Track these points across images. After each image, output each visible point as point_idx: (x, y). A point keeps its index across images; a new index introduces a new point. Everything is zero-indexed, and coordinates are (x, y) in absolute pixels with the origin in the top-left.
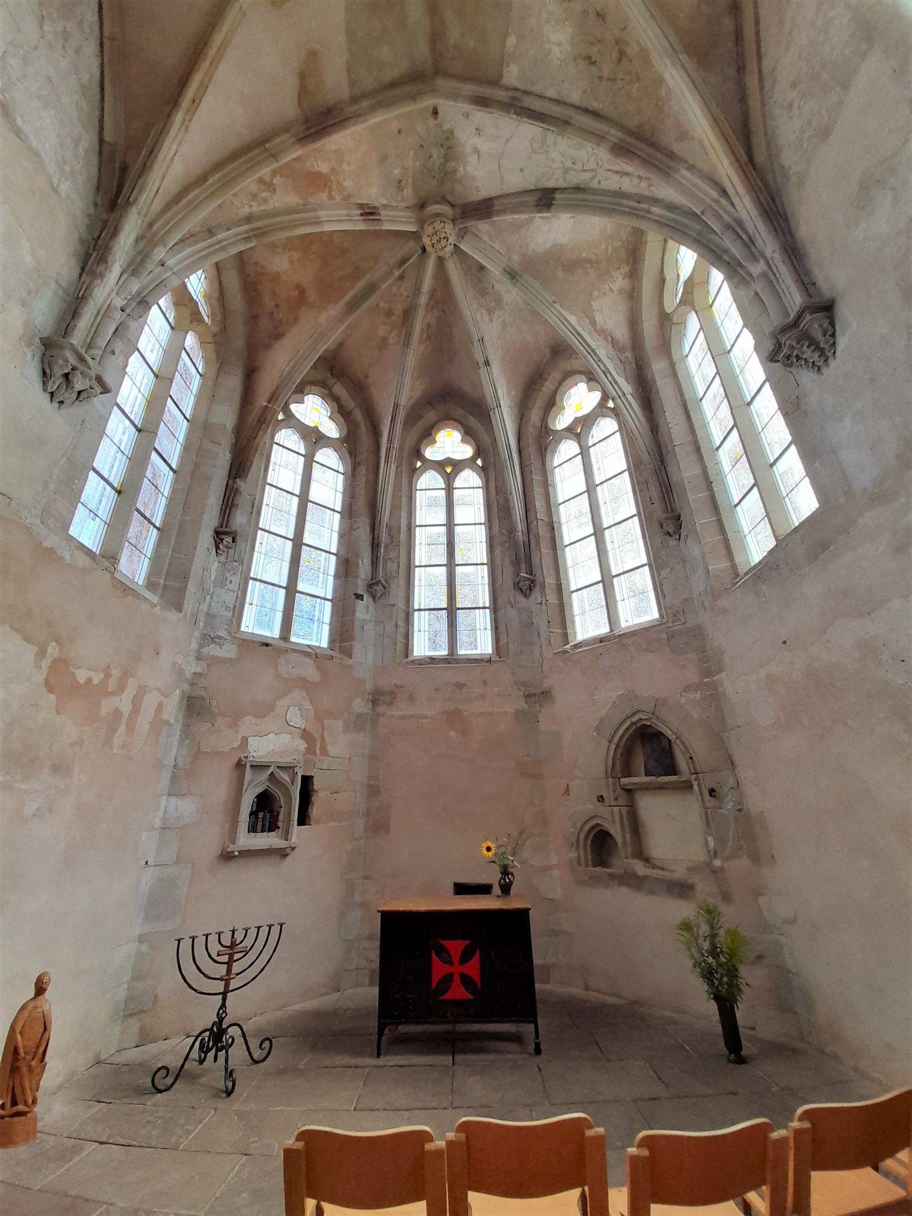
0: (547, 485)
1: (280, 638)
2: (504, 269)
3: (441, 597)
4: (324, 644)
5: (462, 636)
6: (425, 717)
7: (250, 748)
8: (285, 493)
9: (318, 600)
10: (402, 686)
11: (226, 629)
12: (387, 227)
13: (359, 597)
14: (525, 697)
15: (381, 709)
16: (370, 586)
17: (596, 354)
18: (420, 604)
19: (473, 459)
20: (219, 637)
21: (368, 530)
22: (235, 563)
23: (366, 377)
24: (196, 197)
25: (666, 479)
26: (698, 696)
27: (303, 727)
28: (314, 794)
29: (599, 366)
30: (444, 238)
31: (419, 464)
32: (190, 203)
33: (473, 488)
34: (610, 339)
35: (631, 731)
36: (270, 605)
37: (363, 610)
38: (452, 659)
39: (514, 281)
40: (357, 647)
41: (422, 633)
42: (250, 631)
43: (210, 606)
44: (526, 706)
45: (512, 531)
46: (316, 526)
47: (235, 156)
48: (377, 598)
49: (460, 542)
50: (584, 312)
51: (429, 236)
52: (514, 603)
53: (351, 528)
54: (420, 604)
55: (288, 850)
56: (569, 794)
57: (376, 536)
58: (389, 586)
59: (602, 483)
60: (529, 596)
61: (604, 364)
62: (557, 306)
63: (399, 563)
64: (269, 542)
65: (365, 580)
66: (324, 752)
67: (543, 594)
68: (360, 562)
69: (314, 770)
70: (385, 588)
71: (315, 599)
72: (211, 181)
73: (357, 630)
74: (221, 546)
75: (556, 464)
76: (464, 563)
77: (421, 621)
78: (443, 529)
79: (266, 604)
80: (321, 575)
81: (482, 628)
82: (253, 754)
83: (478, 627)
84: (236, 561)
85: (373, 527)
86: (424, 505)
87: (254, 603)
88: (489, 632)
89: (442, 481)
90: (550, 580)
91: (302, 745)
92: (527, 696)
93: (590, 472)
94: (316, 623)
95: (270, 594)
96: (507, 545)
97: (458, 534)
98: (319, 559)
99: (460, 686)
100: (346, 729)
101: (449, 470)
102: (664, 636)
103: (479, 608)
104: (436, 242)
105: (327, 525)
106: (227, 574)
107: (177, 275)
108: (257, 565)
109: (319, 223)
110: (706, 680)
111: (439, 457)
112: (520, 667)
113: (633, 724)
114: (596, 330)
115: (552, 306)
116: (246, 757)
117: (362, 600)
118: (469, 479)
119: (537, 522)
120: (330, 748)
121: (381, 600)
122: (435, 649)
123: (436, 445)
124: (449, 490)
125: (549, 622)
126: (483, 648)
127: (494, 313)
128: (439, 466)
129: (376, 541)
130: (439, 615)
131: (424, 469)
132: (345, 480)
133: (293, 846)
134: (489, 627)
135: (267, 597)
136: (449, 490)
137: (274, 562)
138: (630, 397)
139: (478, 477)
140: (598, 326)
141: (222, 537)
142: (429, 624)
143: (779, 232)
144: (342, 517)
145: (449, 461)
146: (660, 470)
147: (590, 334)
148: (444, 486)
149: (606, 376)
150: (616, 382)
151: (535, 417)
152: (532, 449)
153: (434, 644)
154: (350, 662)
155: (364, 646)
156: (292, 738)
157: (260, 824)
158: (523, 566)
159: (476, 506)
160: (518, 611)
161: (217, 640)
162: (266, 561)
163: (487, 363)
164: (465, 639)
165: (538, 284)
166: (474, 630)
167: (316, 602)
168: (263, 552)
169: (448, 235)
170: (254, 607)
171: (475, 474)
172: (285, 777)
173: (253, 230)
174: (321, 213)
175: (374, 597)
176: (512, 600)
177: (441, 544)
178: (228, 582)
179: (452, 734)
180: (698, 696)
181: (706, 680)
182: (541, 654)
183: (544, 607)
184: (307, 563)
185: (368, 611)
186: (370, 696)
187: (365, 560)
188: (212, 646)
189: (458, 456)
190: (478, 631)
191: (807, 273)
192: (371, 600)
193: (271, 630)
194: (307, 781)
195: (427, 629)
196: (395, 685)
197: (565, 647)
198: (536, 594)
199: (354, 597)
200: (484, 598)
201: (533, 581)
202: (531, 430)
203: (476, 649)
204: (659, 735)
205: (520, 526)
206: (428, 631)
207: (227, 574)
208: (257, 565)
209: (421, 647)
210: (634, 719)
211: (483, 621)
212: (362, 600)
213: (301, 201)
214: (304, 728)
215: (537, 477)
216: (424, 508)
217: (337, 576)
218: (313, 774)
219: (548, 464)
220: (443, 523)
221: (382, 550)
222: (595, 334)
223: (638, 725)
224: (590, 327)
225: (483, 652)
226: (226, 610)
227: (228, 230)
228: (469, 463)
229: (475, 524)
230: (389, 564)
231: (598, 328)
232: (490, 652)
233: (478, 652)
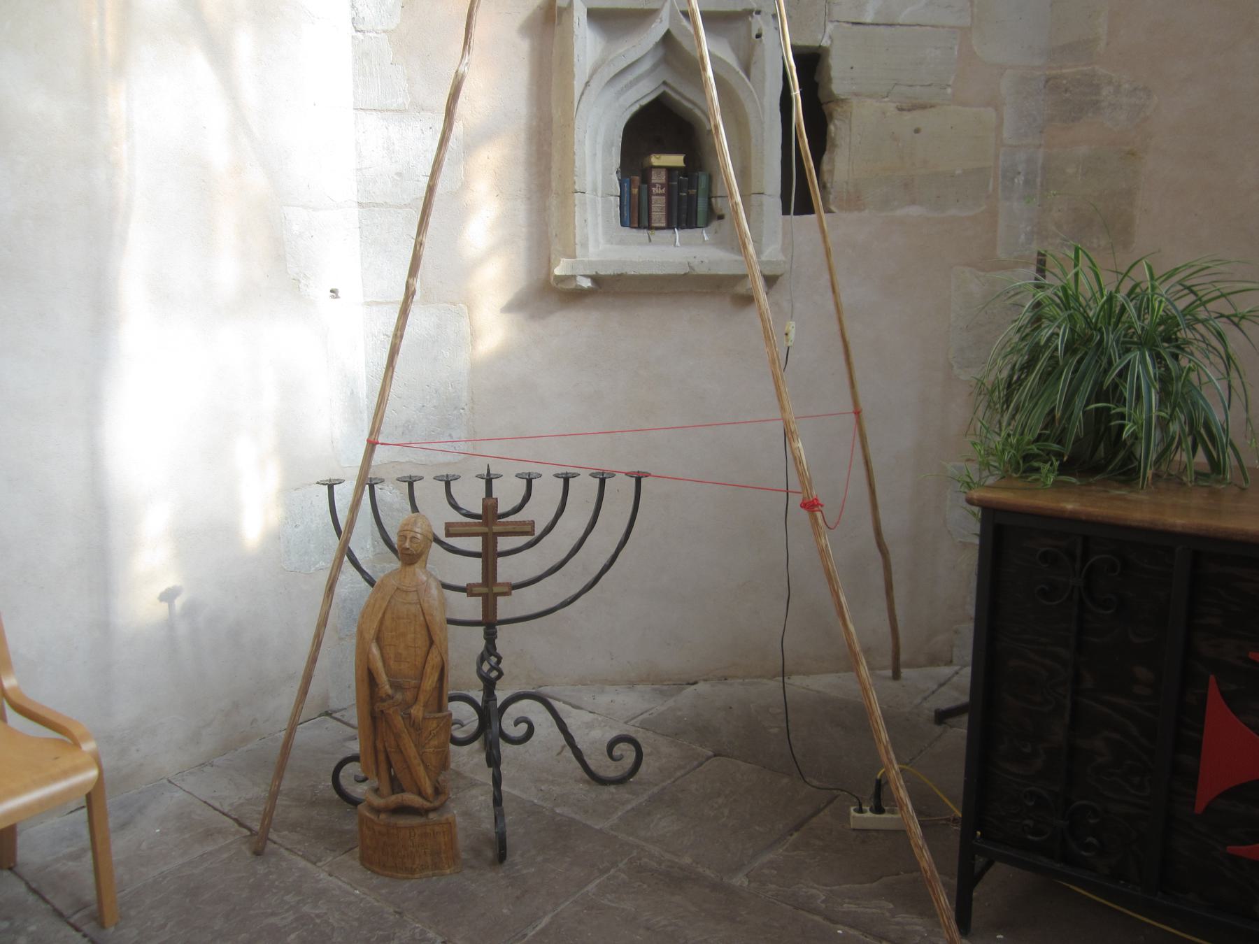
28: (838, 111)
69: (830, 27)
157: (658, 206)
218: (825, 42)
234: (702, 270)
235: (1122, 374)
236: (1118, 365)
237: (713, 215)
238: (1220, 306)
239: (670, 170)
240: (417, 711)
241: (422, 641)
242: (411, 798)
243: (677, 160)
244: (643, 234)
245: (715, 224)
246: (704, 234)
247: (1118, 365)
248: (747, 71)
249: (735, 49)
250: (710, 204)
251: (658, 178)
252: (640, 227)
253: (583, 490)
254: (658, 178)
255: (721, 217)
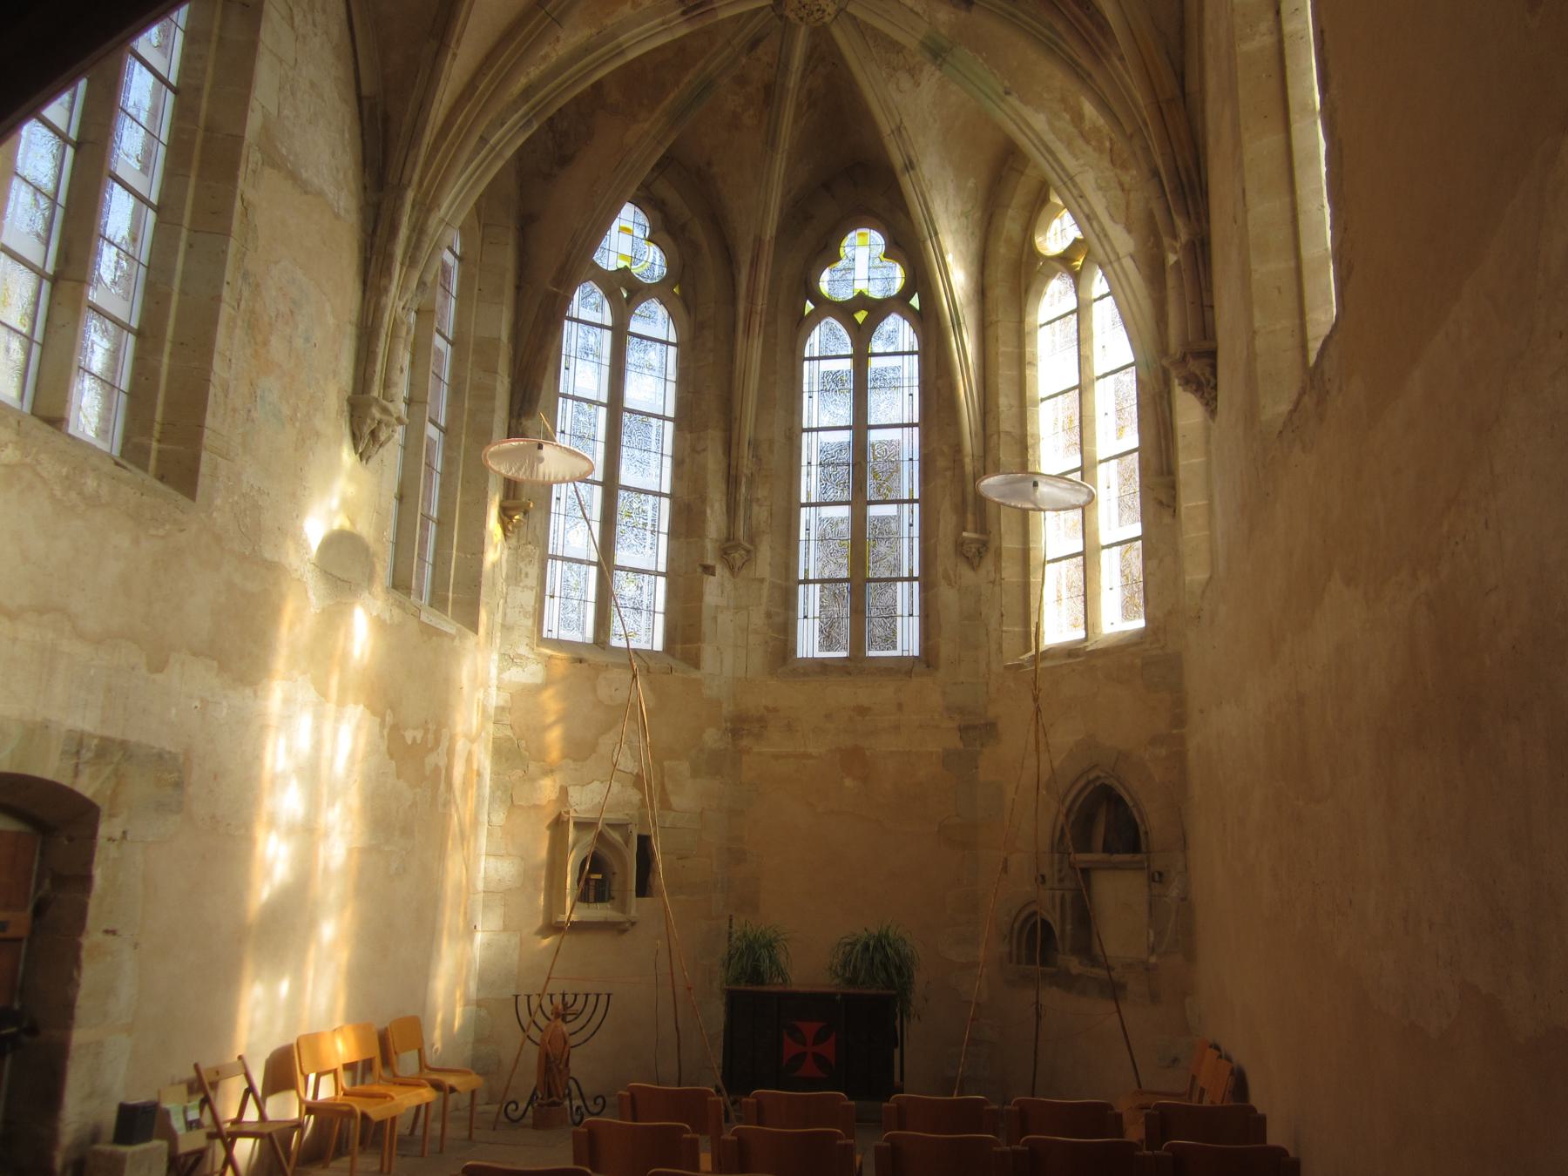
0: (1021, 362)
1: (594, 643)
2: (922, 43)
3: (840, 560)
4: (658, 645)
5: (875, 629)
6: (809, 756)
7: (571, 800)
8: (585, 405)
9: (646, 576)
10: (775, 710)
11: (527, 645)
12: (724, 14)
13: (708, 570)
14: (960, 730)
15: (745, 742)
16: (725, 552)
17: (1075, 185)
18: (807, 571)
19: (905, 295)
20: (520, 656)
21: (720, 452)
22: (530, 547)
23: (709, 164)
24: (466, 119)
25: (1168, 414)
26: (1163, 752)
27: (636, 771)
29: (1080, 206)
30: (818, 10)
31: (809, 306)
32: (461, 128)
33: (903, 354)
34: (1107, 144)
35: (1086, 793)
36: (578, 594)
37: (715, 591)
38: (856, 666)
39: (938, 62)
40: (708, 652)
41: (811, 621)
42: (555, 636)
43: (505, 614)
44: (960, 745)
45: (958, 448)
46: (637, 452)
47: (506, 37)
48: (736, 570)
49: (875, 459)
50: (1063, 100)
51: (792, 10)
52: (952, 577)
53: (694, 450)
54: (807, 571)
55: (627, 925)
56: (1006, 872)
57: (733, 463)
58: (756, 548)
59: (1105, 376)
60: (979, 566)
61: (1088, 202)
62: (1013, 100)
63: (771, 506)
64: (569, 494)
65: (717, 540)
66: (666, 804)
67: (998, 569)
68: (709, 511)
70: (748, 552)
71: (641, 576)
72: (481, 87)
73: (707, 625)
74: (510, 528)
75: (1041, 320)
76: (881, 498)
77: (810, 600)
78: (846, 436)
79: (573, 594)
80: (648, 533)
81: (906, 613)
82: (577, 808)
83: (899, 612)
84: (530, 543)
85: (729, 446)
86: (816, 388)
87: (557, 594)
88: (916, 621)
89: (848, 340)
90: (1010, 543)
91: (635, 796)
92: (964, 730)
93: (1088, 353)
94: (644, 613)
95: (576, 578)
96: (949, 474)
97: (873, 446)
98: (644, 508)
99: (862, 711)
100: (695, 773)
101: (860, 316)
102: (1138, 662)
103: (902, 579)
104: (805, 16)
105: (653, 448)
106: (522, 565)
107: (450, 225)
108: (556, 535)
109: (622, 52)
110: (1174, 732)
111: (844, 294)
112: (955, 684)
113: (1088, 783)
114: (1082, 135)
115: (1003, 101)
116: (568, 813)
117: (714, 575)
118: (897, 333)
119: (999, 437)
120: (675, 800)
121: (744, 572)
122: (829, 649)
123: (839, 265)
124: (861, 357)
125: (1002, 615)
126: (906, 648)
127: (921, 71)
128: (844, 311)
129: (733, 472)
130: (837, 591)
131: (816, 318)
132: (680, 359)
133: (633, 921)
134: (916, 612)
135: (572, 582)
136: (861, 357)
137: (579, 525)
138: (1128, 264)
139: (912, 331)
140: (1087, 122)
141: (512, 513)
142: (821, 607)
143: (1193, 217)
144: (678, 429)
145: (861, 300)
146: (1161, 397)
147: (1069, 145)
148: (850, 351)
149: (1091, 225)
150: (1106, 235)
151: (1011, 225)
152: (999, 291)
153: (828, 640)
154: (695, 674)
155: (718, 649)
156: (622, 786)
157: (592, 893)
158: (970, 517)
159: (906, 390)
160: (959, 590)
161: (518, 661)
162: (567, 526)
163: (910, 166)
164: (878, 631)
165: (980, 60)
166: (892, 617)
167: (643, 580)
168: (562, 512)
169: (824, 7)
170: (557, 600)
171: (907, 323)
172: (616, 836)
173: (533, 108)
174: (622, 39)
175: (731, 568)
176: (951, 573)
177: (843, 463)
178: (523, 576)
179: (848, 782)
180: (1163, 752)
181: (1174, 732)
182: (988, 664)
183: (997, 589)
184: (627, 519)
185: (722, 593)
186: (729, 724)
187: (717, 506)
188: (514, 669)
189: (876, 292)
190: (899, 619)
191: (1210, 290)
192: (727, 574)
193: (583, 633)
194: (644, 842)
195: (817, 614)
196: (766, 708)
197: (1021, 658)
198: (988, 563)
199: (699, 570)
200: (909, 557)
201: (985, 544)
202: (1002, 250)
203: (895, 648)
204: (1119, 800)
205: (969, 443)
206: (820, 618)
207: (522, 565)
208: (556, 535)
209: (808, 643)
210: (1092, 776)
211: (906, 598)
212: (714, 575)
213: (594, 31)
214: (637, 774)
215: (1004, 348)
216: (815, 395)
217: (672, 534)
219: (1028, 320)
220: (848, 424)
221: (743, 490)
222: (1079, 142)
223: (1098, 784)
224: (1071, 129)
225: (906, 654)
226: (525, 616)
227: (502, 125)
228: (898, 303)
229: (902, 426)
230: (755, 508)
231: (1087, 128)
232: (916, 653)
233: (897, 653)
234: (610, 920)
235: (760, 955)
236: (759, 952)
237: (611, 898)
238: (783, 937)
239: (596, 880)
240: (561, 1067)
241: (563, 1042)
242: (555, 1098)
243: (599, 876)
244: (586, 905)
245: (611, 901)
246: (608, 905)
247: (759, 952)
248: (627, 846)
249: (622, 836)
250: (610, 894)
251: (592, 883)
252: (584, 902)
253: (592, 999)
254: (592, 883)
255: (613, 898)
